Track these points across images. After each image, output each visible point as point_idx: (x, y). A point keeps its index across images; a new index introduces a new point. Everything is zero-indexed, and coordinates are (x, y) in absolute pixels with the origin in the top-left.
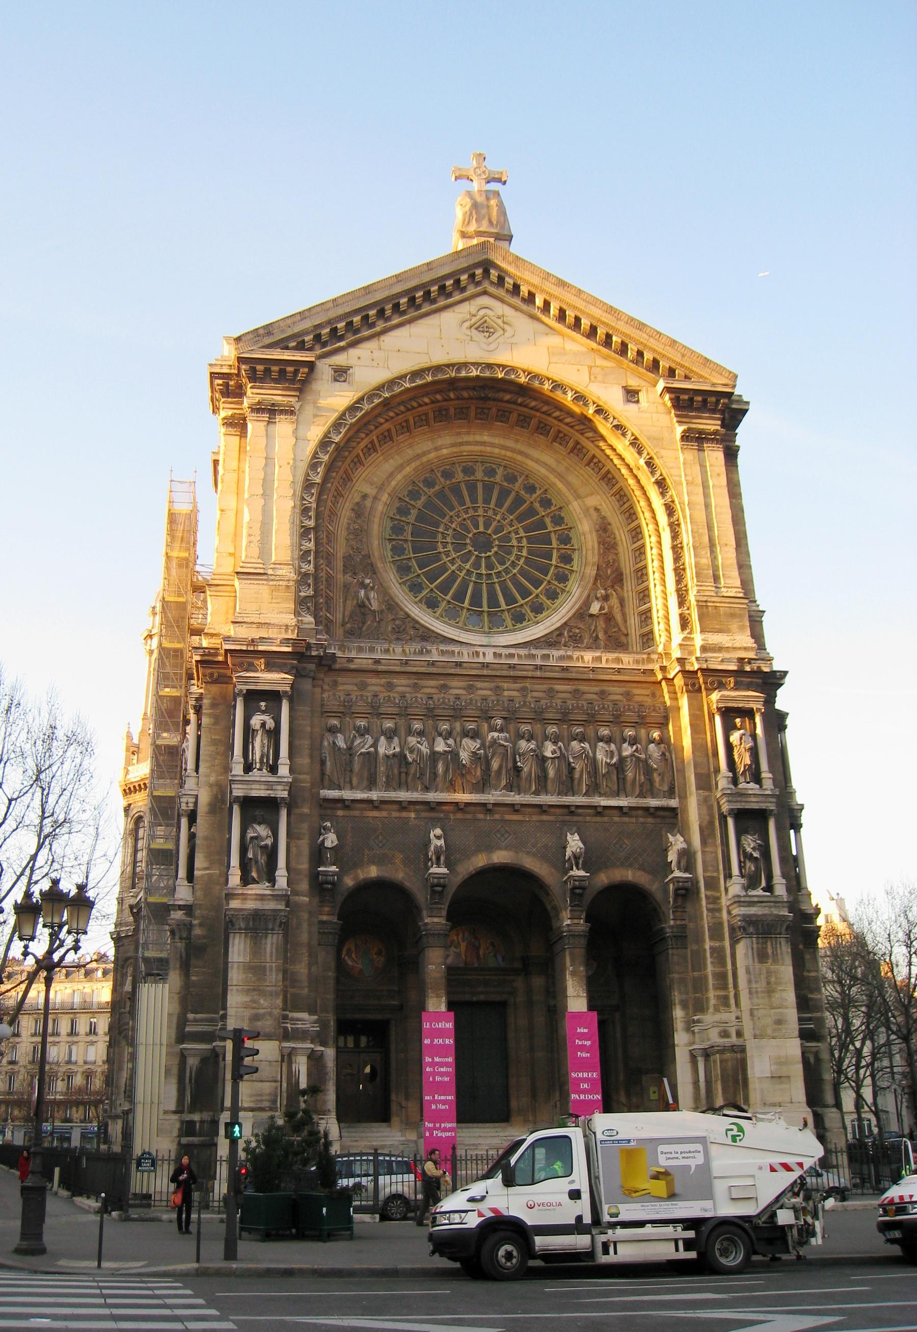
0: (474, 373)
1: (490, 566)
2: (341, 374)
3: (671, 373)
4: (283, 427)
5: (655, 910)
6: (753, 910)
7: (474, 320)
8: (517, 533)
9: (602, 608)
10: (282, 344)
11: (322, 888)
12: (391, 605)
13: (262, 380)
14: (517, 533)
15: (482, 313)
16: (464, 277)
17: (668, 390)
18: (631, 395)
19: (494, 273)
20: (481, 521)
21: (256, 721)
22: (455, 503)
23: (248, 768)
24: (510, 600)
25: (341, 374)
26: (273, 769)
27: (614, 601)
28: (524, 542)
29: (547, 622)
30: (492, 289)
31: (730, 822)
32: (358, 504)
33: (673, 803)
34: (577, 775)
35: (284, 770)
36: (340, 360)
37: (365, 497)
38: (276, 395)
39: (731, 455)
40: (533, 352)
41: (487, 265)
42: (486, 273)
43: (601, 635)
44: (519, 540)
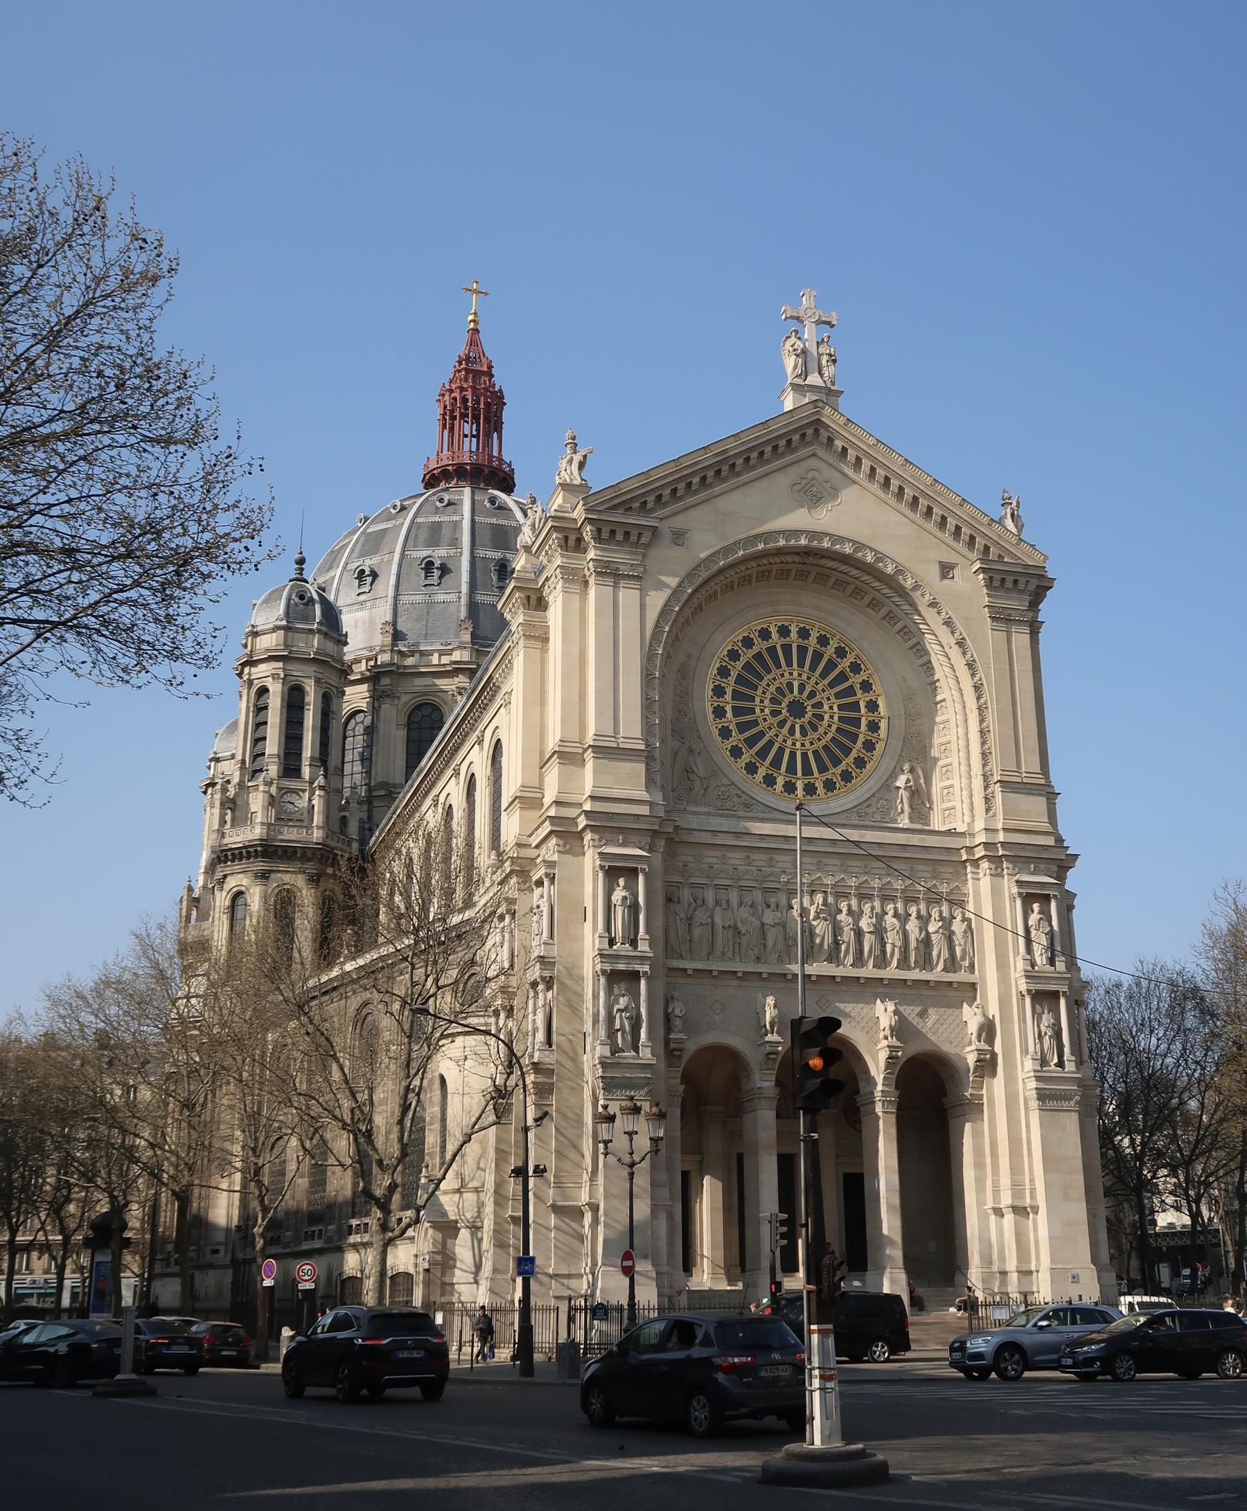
0: (803, 542)
1: (804, 733)
2: (679, 537)
5: (953, 1076)
6: (1042, 1085)
7: (804, 482)
8: (828, 699)
9: (908, 781)
10: (626, 506)
11: (670, 1052)
12: (715, 771)
13: (606, 542)
14: (828, 699)
15: (811, 474)
16: (796, 438)
17: (983, 570)
18: (946, 570)
19: (824, 433)
20: (796, 684)
21: (618, 895)
22: (772, 666)
23: (612, 942)
25: (679, 537)
26: (634, 943)
28: (835, 709)
29: (858, 792)
30: (821, 452)
31: (1028, 1000)
32: (683, 665)
36: (678, 522)
37: (689, 656)
38: (621, 557)
39: (1034, 628)
40: (853, 517)
41: (817, 425)
42: (816, 430)
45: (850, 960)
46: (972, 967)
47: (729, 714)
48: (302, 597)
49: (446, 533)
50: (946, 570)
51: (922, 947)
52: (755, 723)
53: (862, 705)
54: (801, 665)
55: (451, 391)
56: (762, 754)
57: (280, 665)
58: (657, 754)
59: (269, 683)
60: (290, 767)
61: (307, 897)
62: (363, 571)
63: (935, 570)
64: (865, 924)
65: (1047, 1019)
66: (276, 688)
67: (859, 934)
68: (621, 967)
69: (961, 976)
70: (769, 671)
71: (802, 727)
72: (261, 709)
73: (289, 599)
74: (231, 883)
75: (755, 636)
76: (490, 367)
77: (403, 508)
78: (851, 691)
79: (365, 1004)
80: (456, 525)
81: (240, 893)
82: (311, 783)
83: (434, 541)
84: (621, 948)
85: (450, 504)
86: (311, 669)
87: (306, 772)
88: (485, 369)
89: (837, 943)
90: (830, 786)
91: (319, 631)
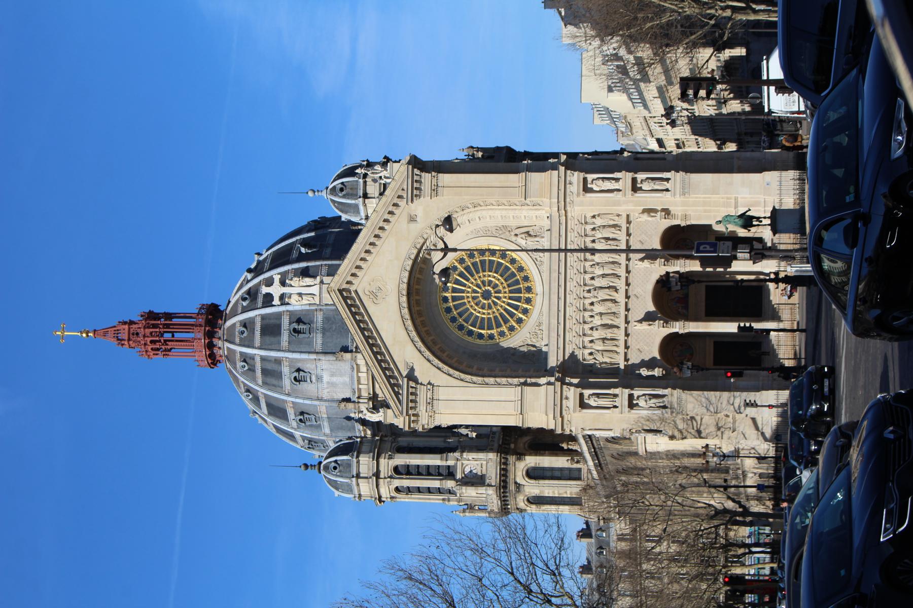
1: (499, 292)
3: (400, 197)
4: (442, 393)
18: (412, 219)
22: (464, 307)
23: (615, 407)
24: (517, 282)
26: (616, 396)
27: (517, 231)
29: (529, 264)
33: (624, 217)
34: (611, 260)
35: (617, 391)
42: (344, 290)
43: (537, 239)
44: (484, 276)
45: (616, 280)
46: (618, 215)
47: (492, 332)
48: (335, 468)
49: (269, 366)
50: (412, 219)
51: (609, 242)
52: (495, 317)
53: (482, 258)
54: (463, 291)
55: (147, 351)
56: (512, 315)
57: (381, 481)
58: (522, 380)
59: (393, 487)
60: (450, 473)
61: (531, 461)
62: (301, 420)
63: (412, 225)
64: (598, 271)
65: (645, 186)
66: (397, 483)
67: (604, 276)
68: (627, 403)
69: (623, 222)
70: (467, 309)
71: (496, 292)
72: (409, 490)
73: (337, 476)
74: (522, 505)
75: (449, 316)
76: (125, 323)
77: (248, 391)
78: (474, 264)
79: (612, 456)
80: (263, 359)
81: (528, 500)
82: (457, 460)
83: (279, 375)
84: (618, 402)
85: (245, 361)
86: (383, 461)
87: (451, 463)
88: (126, 327)
89: (609, 287)
90: (526, 279)
91: (358, 457)
